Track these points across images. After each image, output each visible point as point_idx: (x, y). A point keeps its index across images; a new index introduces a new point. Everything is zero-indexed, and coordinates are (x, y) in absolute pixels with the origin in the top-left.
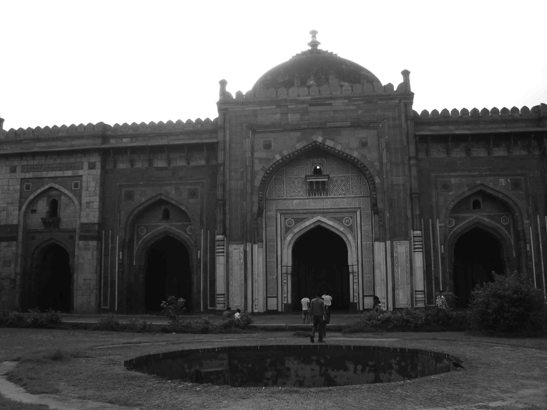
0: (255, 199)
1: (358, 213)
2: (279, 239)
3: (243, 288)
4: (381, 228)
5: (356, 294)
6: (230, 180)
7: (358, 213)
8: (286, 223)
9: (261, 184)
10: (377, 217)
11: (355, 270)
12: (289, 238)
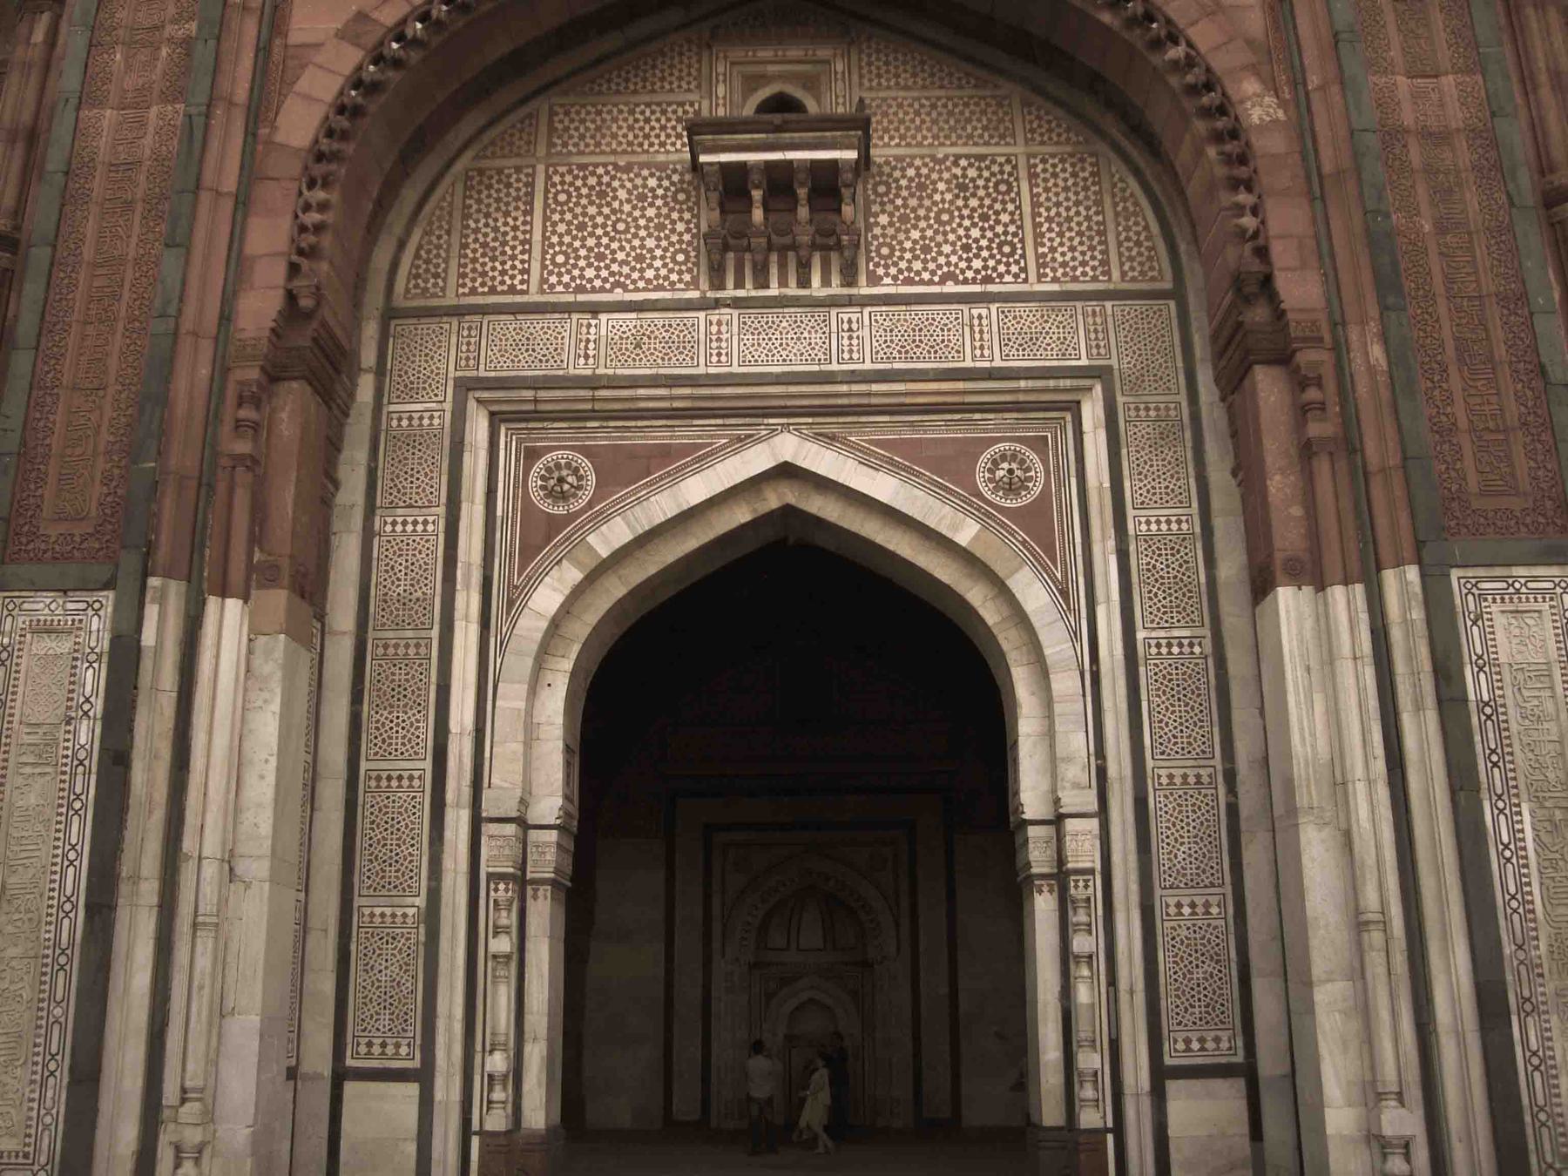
0: (269, 237)
1: (1092, 412)
2: (468, 602)
3: (66, 985)
4: (1322, 466)
5: (1091, 1060)
6: (87, 97)
7: (1092, 412)
8: (534, 482)
9: (330, 133)
10: (1268, 386)
11: (1082, 846)
12: (547, 598)
